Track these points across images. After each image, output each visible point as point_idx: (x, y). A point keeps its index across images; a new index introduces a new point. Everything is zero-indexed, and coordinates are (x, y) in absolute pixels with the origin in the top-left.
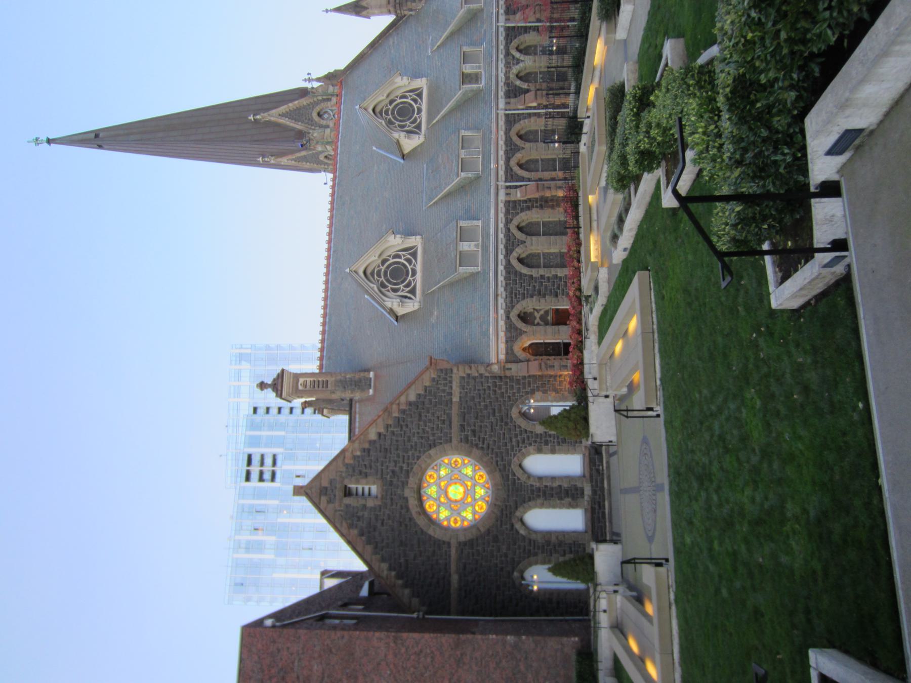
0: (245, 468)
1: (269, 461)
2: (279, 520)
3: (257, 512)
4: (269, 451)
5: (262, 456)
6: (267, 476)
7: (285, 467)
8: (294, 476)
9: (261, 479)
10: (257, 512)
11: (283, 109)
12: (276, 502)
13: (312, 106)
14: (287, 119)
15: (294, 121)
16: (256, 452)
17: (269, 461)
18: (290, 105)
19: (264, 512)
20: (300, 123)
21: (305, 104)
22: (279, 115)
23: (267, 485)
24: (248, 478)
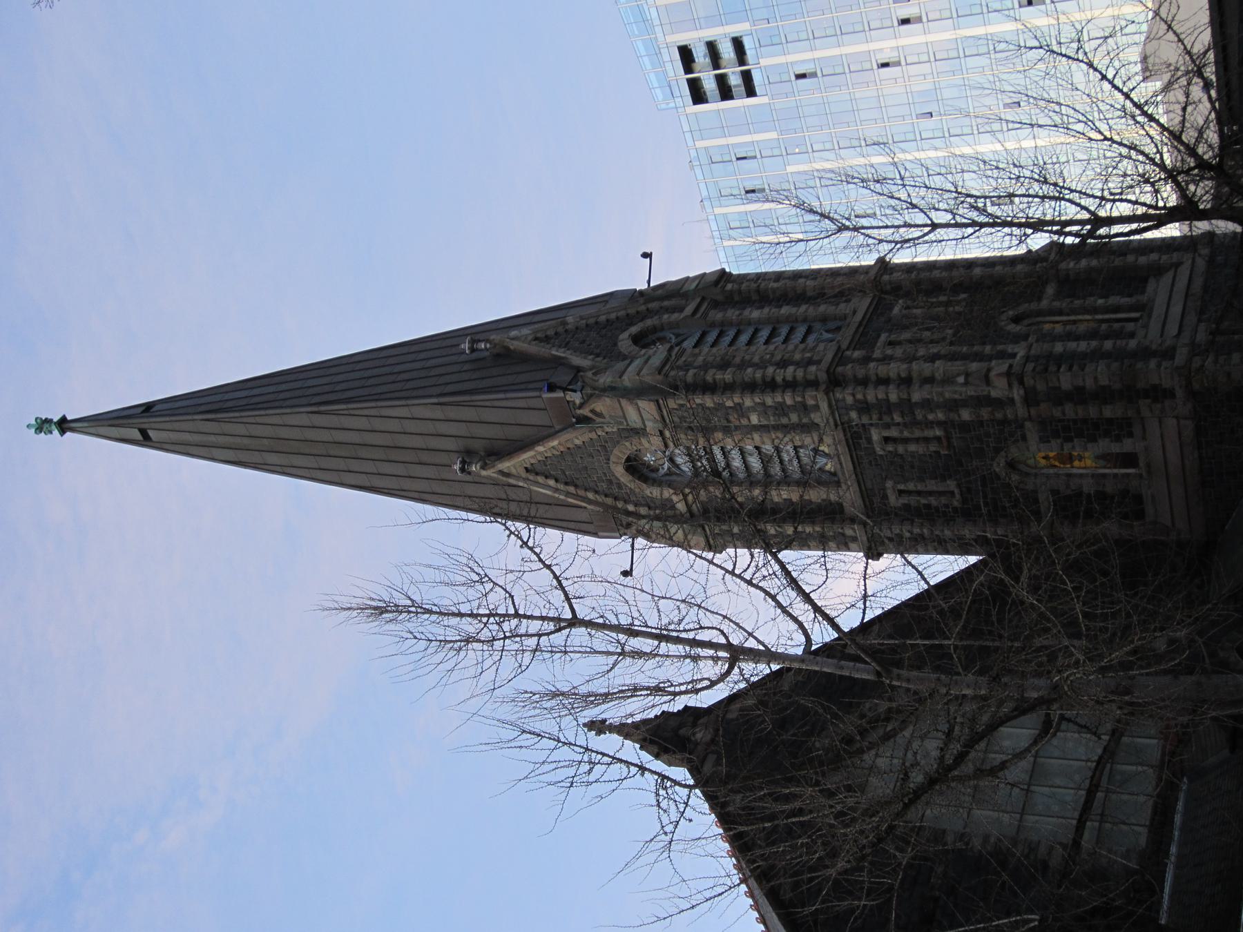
0: (683, 77)
1: (727, 51)
2: (790, 169)
3: (738, 159)
4: (722, 34)
5: (712, 47)
6: (735, 80)
7: (763, 62)
8: (793, 78)
9: (726, 93)
10: (738, 159)
11: (527, 457)
12: (773, 135)
13: (605, 447)
14: (552, 482)
15: (572, 489)
16: (696, 39)
17: (727, 51)
18: (540, 449)
19: (755, 157)
20: (590, 495)
21: (577, 442)
22: (527, 470)
23: (740, 103)
24: (698, 96)
